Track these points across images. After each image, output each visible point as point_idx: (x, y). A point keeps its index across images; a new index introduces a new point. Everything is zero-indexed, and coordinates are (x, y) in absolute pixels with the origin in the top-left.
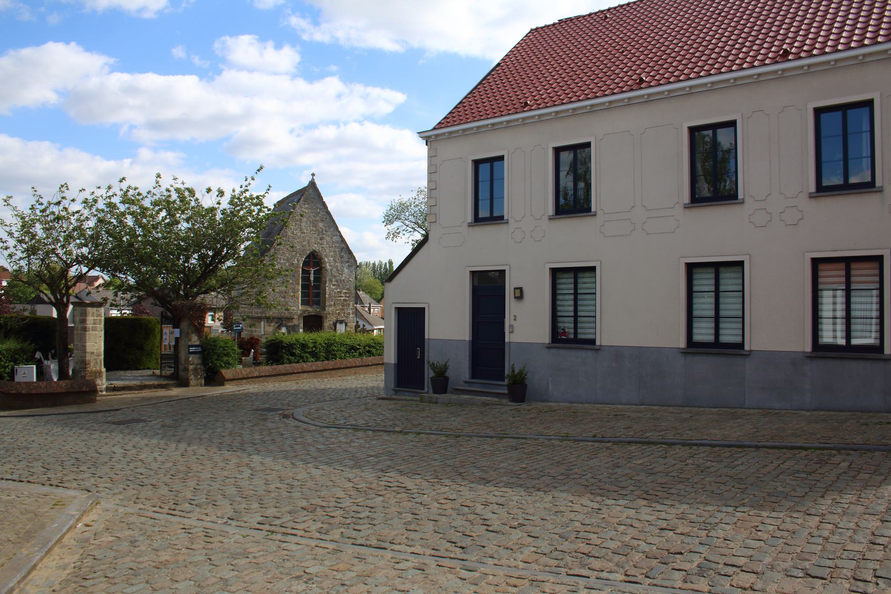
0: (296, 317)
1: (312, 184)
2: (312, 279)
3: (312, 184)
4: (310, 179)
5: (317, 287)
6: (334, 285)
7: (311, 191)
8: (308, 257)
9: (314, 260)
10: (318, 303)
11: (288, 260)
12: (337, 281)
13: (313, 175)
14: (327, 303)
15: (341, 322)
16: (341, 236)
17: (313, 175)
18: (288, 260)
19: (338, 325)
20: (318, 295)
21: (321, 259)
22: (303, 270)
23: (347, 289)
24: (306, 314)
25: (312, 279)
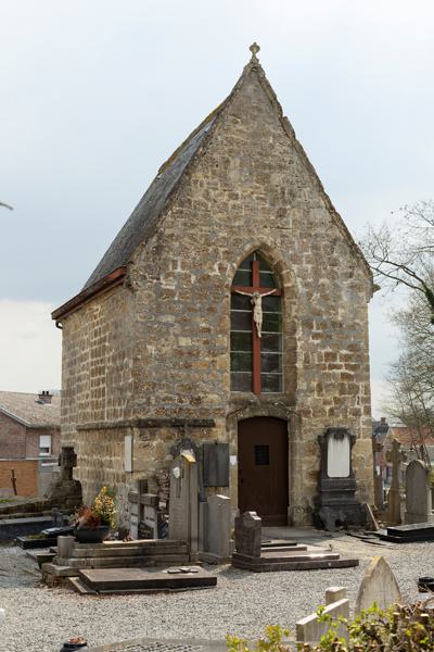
0: (220, 422)
1: (254, 71)
2: (258, 318)
3: (254, 71)
4: (247, 57)
5: (271, 343)
6: (316, 336)
7: (250, 88)
8: (248, 262)
9: (260, 270)
10: (274, 384)
11: (196, 267)
12: (323, 325)
13: (255, 48)
14: (302, 385)
15: (340, 434)
16: (331, 209)
17: (255, 48)
18: (196, 267)
19: (332, 444)
20: (274, 363)
21: (278, 268)
22: (234, 294)
23: (352, 347)
24: (246, 414)
25: (258, 318)
